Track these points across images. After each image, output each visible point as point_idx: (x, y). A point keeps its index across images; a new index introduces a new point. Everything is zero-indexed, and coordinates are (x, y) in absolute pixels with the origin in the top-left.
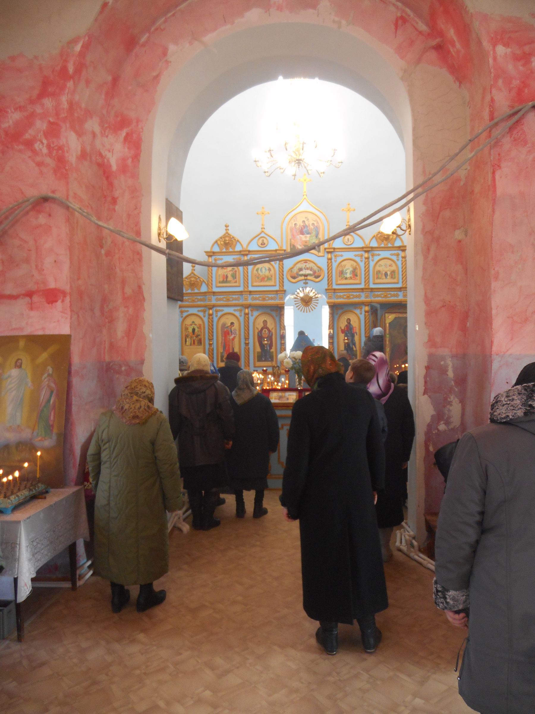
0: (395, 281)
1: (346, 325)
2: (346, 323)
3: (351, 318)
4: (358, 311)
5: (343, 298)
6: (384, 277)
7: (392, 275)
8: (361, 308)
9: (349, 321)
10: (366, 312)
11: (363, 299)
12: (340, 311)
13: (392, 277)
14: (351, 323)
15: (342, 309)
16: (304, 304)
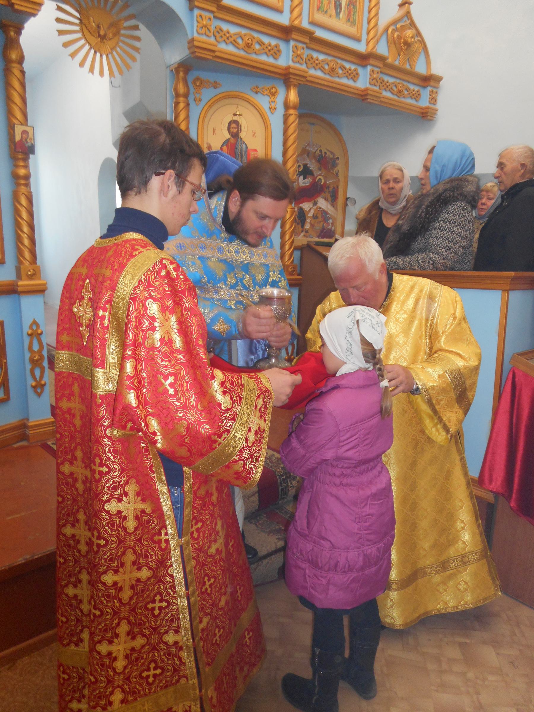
0: (352, 30)
1: (227, 142)
2: (228, 136)
3: (243, 122)
4: (263, 101)
5: (235, 44)
6: (334, 13)
7: (349, 13)
8: (273, 94)
9: (234, 128)
10: (287, 106)
11: (285, 60)
12: (207, 94)
13: (348, 19)
14: (243, 135)
15: (216, 85)
16: (94, 41)
